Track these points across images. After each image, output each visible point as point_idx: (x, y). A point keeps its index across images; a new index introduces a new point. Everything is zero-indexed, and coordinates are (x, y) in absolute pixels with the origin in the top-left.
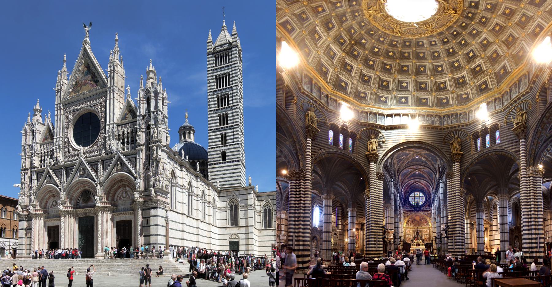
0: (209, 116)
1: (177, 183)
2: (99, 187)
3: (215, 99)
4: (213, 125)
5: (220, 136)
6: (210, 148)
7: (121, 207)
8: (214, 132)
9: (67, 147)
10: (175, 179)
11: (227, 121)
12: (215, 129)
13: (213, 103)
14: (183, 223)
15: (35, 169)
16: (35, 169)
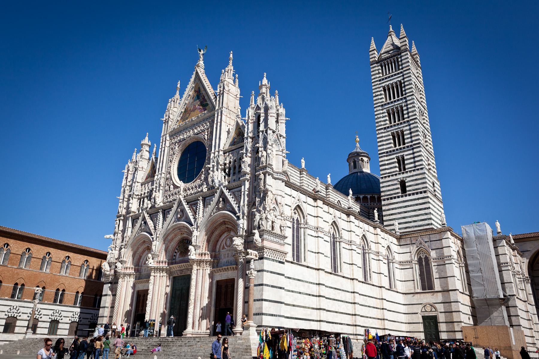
0: (378, 136)
1: (307, 223)
2: (195, 233)
3: (384, 115)
4: (385, 147)
5: (396, 160)
6: (382, 178)
7: (224, 260)
8: (387, 156)
9: (168, 185)
10: (304, 218)
11: (404, 140)
12: (387, 152)
13: (382, 119)
14: (319, 284)
15: (131, 215)
16: (131, 215)
